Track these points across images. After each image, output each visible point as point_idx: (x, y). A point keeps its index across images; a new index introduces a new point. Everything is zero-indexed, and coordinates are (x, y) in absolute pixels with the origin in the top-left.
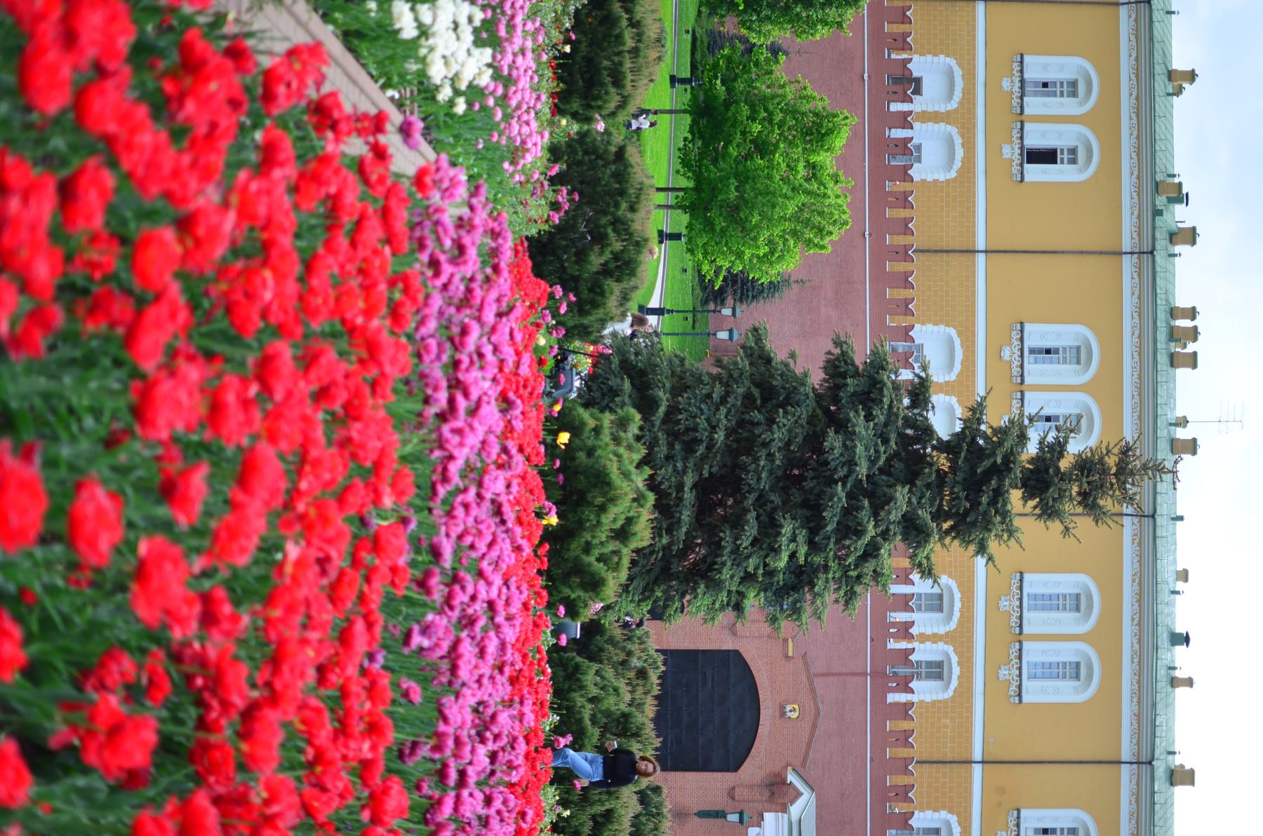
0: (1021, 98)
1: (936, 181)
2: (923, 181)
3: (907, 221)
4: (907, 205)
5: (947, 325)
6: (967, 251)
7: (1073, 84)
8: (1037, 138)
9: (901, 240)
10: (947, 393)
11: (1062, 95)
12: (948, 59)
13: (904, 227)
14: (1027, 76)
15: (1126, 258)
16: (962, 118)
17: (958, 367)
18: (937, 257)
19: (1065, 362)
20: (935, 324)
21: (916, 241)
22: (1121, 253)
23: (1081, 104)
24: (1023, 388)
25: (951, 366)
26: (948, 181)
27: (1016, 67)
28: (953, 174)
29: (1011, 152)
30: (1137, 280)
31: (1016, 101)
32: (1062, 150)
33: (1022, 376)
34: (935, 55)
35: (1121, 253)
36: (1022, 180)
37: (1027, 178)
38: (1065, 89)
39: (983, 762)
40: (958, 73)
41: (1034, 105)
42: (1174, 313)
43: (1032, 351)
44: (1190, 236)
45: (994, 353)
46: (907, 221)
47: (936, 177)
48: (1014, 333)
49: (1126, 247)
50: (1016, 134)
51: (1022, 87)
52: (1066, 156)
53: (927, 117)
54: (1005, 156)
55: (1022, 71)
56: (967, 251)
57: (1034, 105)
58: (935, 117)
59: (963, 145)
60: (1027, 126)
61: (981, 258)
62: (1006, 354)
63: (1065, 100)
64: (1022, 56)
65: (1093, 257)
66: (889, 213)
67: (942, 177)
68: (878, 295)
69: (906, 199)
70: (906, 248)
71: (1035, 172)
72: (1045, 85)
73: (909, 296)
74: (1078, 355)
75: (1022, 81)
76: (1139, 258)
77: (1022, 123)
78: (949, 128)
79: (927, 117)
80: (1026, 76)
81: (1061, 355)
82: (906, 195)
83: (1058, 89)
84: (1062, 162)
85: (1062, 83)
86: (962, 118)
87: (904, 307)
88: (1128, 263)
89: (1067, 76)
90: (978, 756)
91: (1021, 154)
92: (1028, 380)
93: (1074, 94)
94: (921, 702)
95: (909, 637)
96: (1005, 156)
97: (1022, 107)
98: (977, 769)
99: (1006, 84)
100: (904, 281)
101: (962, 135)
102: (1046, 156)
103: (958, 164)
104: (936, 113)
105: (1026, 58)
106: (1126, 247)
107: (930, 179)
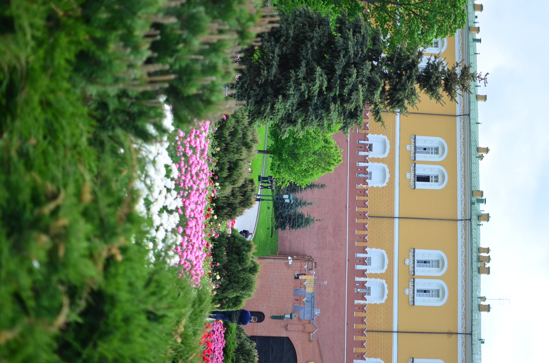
0: (415, 153)
1: (377, 187)
2: (372, 187)
3: (365, 201)
4: (365, 195)
5: (382, 249)
6: (391, 217)
7: (437, 149)
8: (421, 171)
9: (361, 326)
10: (381, 278)
11: (432, 153)
12: (384, 136)
13: (364, 204)
14: (417, 144)
15: (459, 222)
16: (389, 161)
17: (386, 297)
18: (378, 219)
19: (433, 296)
20: (377, 248)
21: (367, 327)
22: (457, 220)
23: (440, 157)
24: (414, 277)
25: (383, 267)
26: (383, 187)
27: (413, 140)
28: (385, 185)
29: (410, 176)
30: (464, 232)
31: (412, 155)
32: (432, 177)
33: (414, 272)
34: (378, 134)
35: (457, 220)
36: (415, 188)
37: (417, 187)
38: (433, 151)
39: (398, 332)
40: (388, 142)
41: (420, 157)
42: (480, 250)
43: (418, 291)
44: (487, 217)
45: (402, 261)
46: (365, 201)
47: (378, 185)
48: (410, 253)
49: (459, 217)
50: (412, 169)
51: (415, 149)
52: (433, 179)
53: (374, 160)
54: (408, 178)
55: (415, 142)
56: (391, 217)
57: (420, 157)
58: (378, 160)
59: (389, 172)
60: (417, 165)
61: (395, 335)
62: (407, 262)
63: (433, 155)
64: (415, 136)
65: (445, 222)
66: (356, 244)
67: (378, 302)
68: (352, 233)
69: (365, 192)
70: (363, 330)
71: (420, 185)
72: (425, 149)
73: (363, 316)
74: (438, 264)
75: (415, 146)
76: (465, 222)
77: (415, 164)
78: (384, 165)
79: (374, 160)
80: (417, 145)
81: (431, 264)
82: (365, 190)
83: (430, 151)
84: (432, 181)
85: (432, 148)
86: (389, 161)
87: (363, 239)
88: (460, 224)
89: (434, 145)
90: (395, 329)
91: (414, 177)
92: (416, 274)
93: (437, 153)
94: (370, 304)
95: (365, 217)
96: (408, 178)
97: (415, 157)
98: (395, 335)
99: (408, 147)
100: (361, 344)
101: (389, 168)
102: (426, 179)
103: (387, 180)
104: (376, 274)
105: (417, 137)
106: (459, 217)
107: (375, 186)
